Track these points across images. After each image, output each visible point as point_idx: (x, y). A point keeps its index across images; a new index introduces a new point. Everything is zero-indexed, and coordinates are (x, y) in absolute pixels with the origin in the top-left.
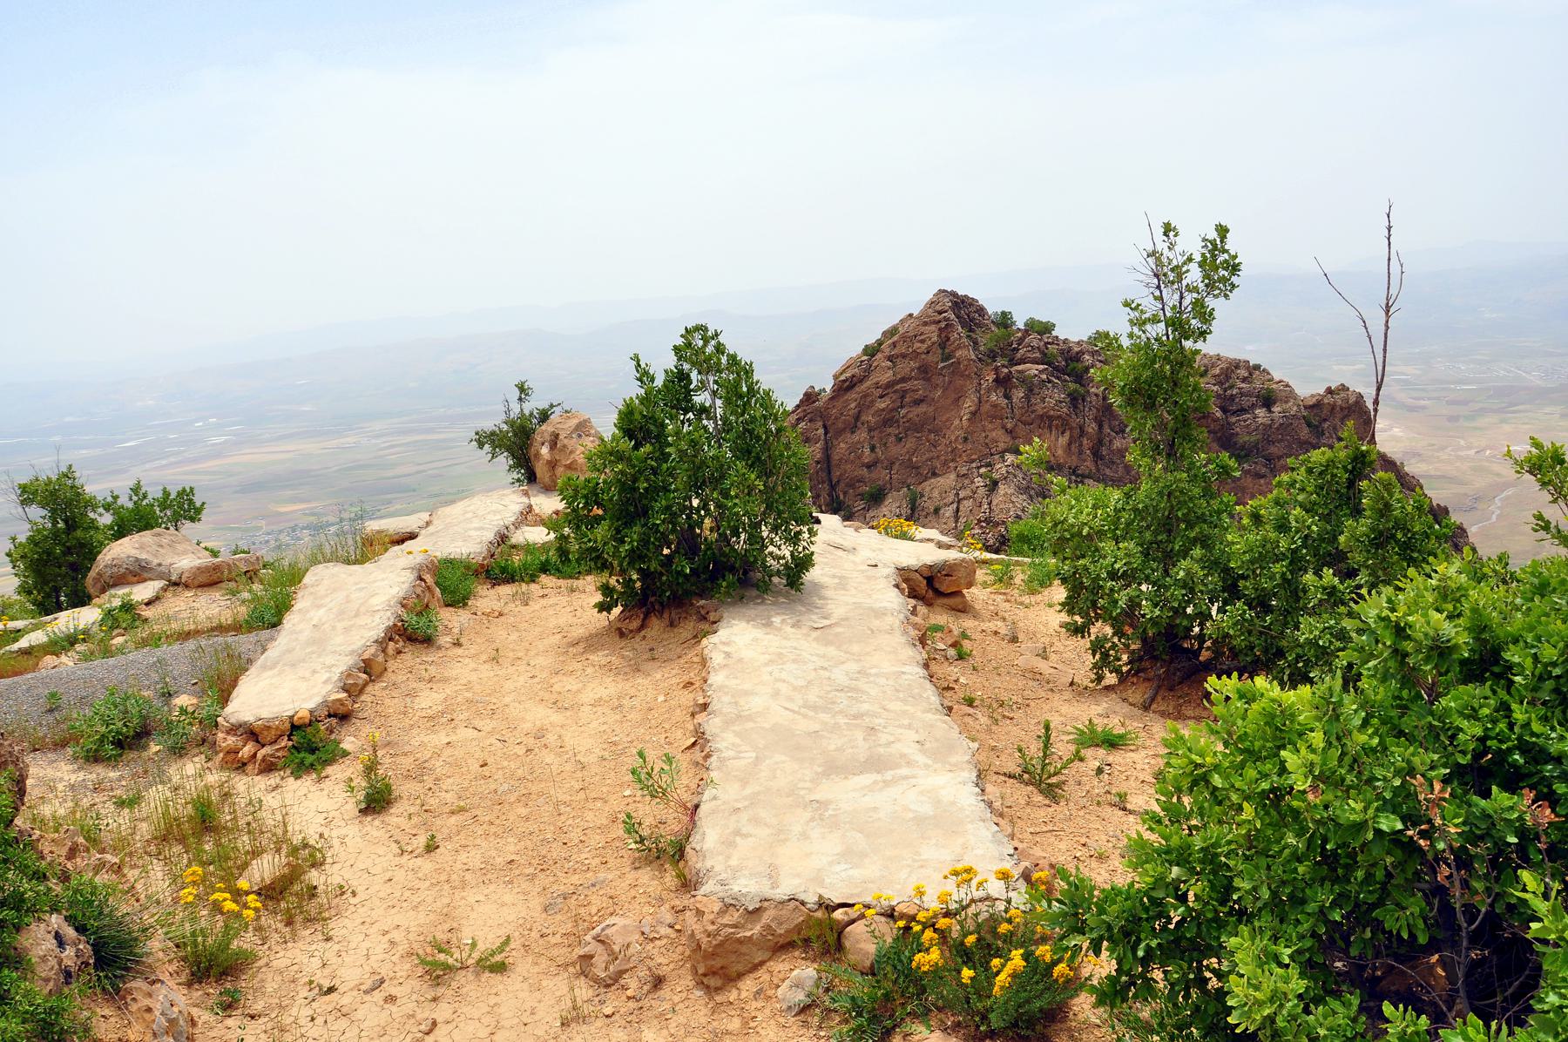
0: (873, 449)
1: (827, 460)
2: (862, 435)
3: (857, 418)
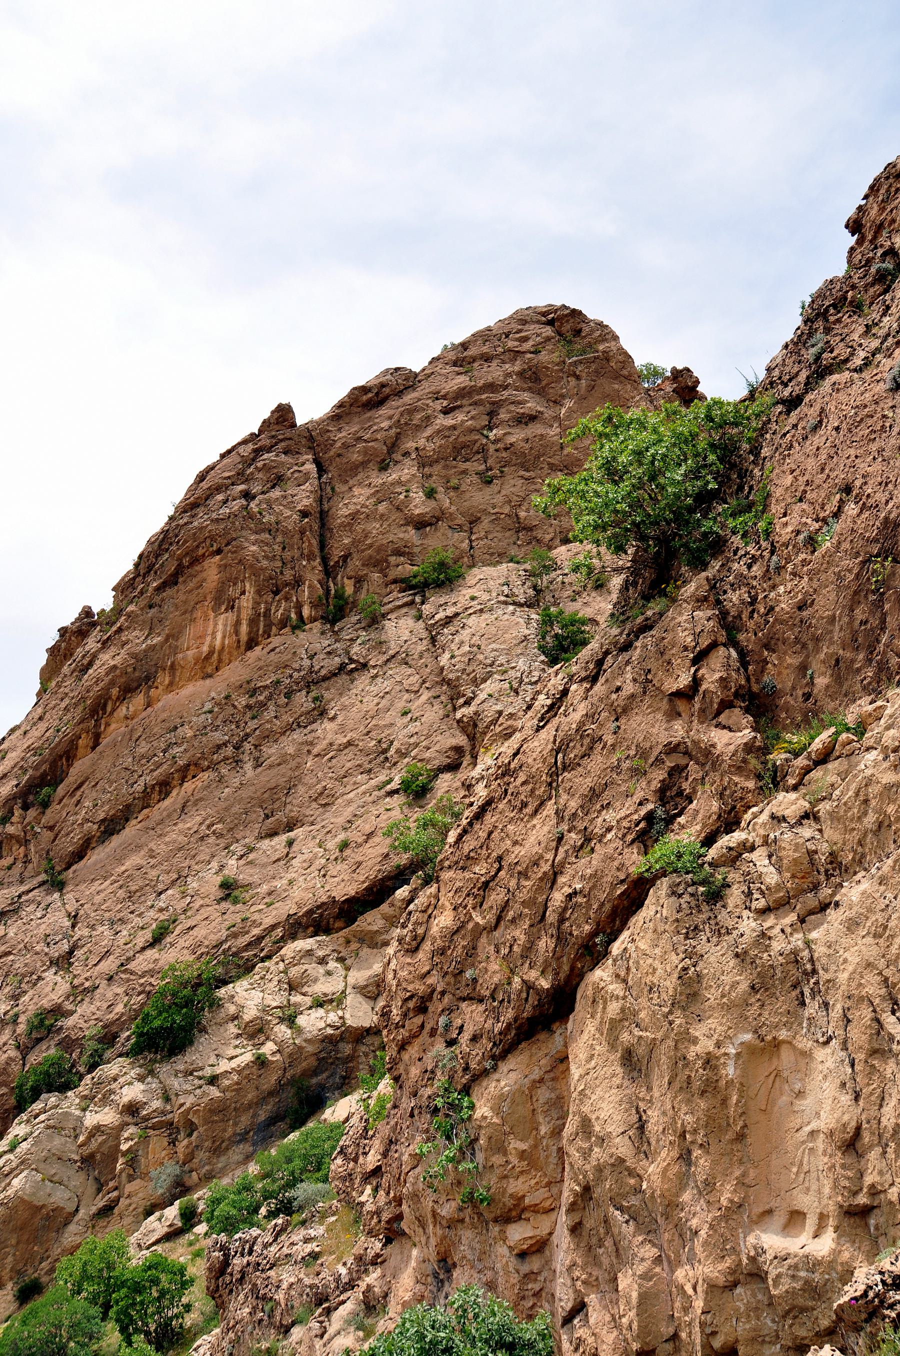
0: (430, 494)
1: (321, 516)
2: (406, 471)
3: (393, 446)
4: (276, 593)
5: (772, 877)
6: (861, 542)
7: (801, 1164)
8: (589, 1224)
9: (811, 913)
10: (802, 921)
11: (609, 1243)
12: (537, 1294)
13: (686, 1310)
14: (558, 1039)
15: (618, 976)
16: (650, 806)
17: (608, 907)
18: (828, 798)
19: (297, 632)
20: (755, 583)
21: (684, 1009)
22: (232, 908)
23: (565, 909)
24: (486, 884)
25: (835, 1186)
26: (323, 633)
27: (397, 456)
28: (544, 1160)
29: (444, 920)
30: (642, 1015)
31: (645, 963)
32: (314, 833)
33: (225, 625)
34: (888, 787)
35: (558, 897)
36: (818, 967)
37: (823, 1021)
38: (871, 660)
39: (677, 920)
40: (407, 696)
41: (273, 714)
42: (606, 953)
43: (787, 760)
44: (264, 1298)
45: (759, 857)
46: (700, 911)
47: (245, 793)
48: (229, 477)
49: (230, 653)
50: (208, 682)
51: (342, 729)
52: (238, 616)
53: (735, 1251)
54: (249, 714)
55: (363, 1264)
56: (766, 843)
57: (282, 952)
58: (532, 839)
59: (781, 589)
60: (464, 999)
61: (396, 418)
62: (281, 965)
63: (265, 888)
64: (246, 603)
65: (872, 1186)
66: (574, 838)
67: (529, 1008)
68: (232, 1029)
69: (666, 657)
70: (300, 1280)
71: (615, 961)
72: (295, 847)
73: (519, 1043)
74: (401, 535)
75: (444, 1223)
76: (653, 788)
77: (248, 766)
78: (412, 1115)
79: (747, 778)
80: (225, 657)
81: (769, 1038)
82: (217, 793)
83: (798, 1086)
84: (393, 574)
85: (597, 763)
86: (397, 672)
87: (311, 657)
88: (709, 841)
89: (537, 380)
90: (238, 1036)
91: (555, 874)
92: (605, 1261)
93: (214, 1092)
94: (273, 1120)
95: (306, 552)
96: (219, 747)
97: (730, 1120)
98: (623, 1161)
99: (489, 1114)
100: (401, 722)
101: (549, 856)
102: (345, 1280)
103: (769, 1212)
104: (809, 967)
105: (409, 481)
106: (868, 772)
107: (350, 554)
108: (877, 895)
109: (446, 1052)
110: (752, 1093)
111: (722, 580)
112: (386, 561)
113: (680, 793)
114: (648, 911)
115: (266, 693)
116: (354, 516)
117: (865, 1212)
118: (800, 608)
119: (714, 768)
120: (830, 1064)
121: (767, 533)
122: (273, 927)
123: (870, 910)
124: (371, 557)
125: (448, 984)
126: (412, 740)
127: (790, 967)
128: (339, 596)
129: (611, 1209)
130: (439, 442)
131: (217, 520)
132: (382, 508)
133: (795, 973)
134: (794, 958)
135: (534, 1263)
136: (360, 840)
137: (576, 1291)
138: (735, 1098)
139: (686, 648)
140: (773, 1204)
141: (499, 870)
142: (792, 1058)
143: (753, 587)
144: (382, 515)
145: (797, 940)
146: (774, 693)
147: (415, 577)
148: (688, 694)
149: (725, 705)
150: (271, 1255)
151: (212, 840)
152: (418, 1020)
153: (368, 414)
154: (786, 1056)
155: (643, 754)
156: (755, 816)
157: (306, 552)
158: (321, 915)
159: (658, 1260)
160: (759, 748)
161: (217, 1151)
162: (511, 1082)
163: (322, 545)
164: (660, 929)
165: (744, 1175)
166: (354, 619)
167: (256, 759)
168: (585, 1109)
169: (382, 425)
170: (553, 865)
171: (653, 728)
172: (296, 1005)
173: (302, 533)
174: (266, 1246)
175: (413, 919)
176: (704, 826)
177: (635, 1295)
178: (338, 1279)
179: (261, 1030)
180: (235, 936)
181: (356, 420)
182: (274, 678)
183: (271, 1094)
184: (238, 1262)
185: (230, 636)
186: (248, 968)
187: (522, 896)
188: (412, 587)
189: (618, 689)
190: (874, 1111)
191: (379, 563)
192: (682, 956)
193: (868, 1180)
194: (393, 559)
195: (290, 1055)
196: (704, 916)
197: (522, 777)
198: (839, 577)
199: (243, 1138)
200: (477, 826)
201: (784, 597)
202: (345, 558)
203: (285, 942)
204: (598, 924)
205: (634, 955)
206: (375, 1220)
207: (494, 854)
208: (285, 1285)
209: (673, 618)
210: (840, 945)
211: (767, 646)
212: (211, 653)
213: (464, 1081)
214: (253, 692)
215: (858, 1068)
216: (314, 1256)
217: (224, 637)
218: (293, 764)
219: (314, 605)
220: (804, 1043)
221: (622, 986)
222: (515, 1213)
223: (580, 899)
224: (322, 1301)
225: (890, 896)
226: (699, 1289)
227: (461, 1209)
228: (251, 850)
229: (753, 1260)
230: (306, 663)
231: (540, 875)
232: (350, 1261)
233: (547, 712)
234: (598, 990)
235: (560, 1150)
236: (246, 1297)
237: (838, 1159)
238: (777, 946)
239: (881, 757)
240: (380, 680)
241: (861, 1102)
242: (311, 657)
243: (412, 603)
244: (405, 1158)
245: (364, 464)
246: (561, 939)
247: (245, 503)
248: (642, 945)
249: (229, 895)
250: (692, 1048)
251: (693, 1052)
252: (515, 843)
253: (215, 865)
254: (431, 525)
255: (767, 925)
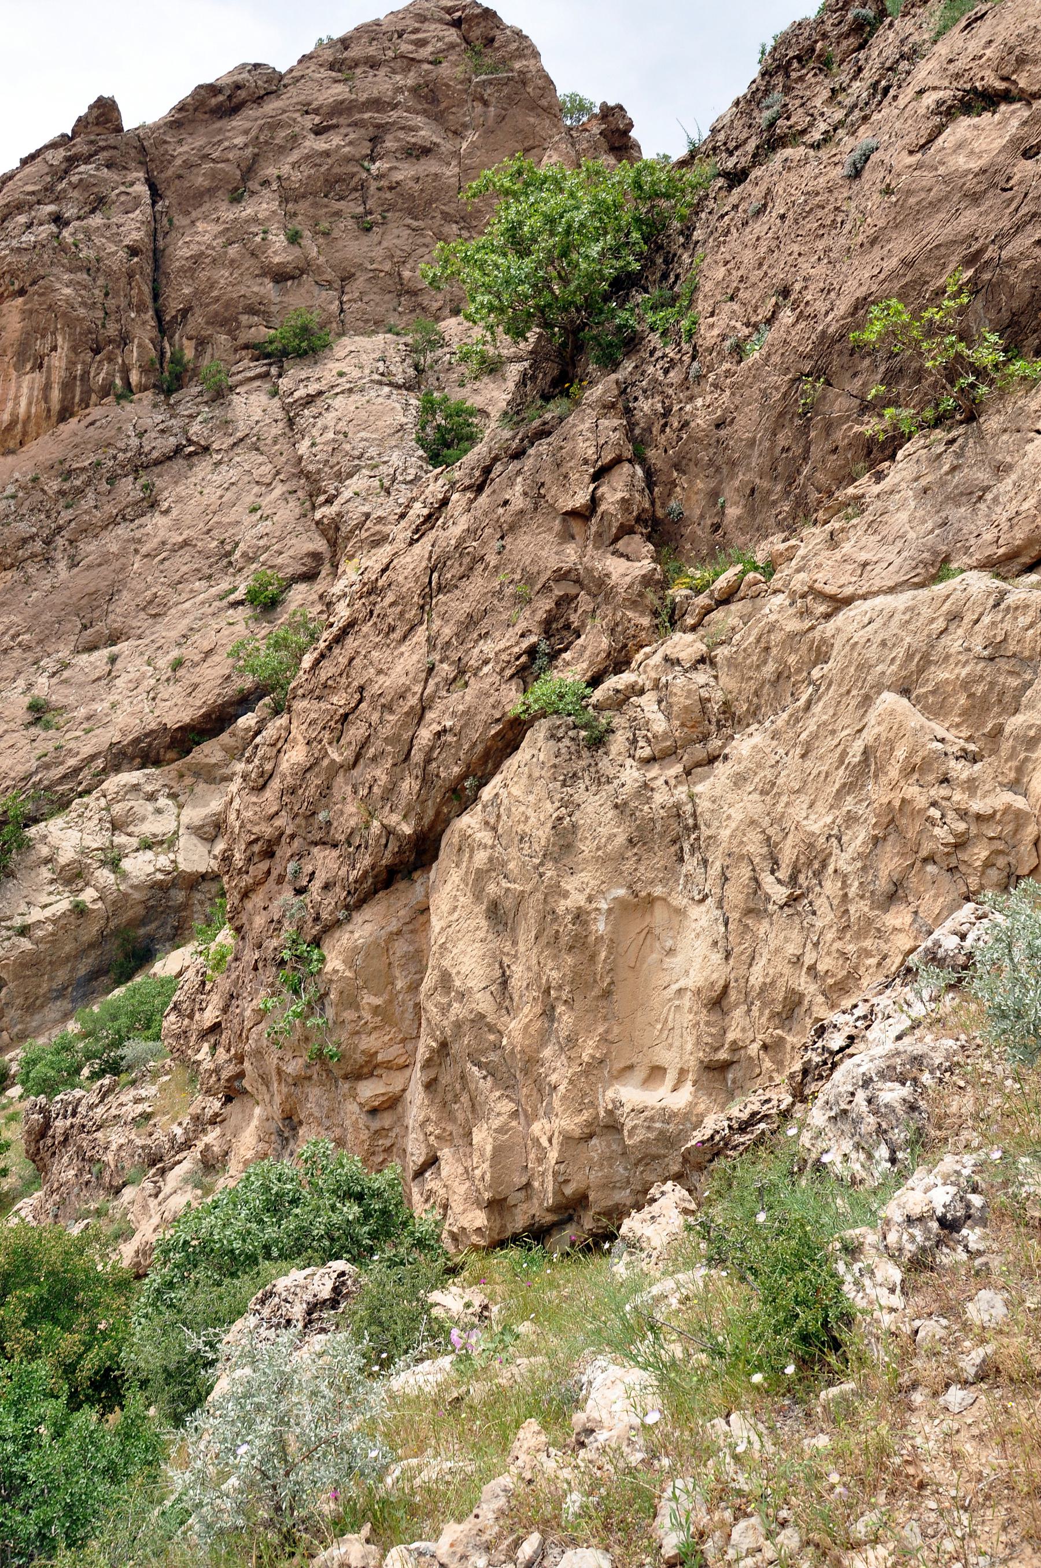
0: (294, 238)
1: (154, 255)
2: (263, 205)
4: (97, 351)
5: (659, 724)
6: (793, 357)
7: (666, 1021)
8: (445, 1079)
9: (698, 765)
10: (688, 773)
11: (465, 1098)
12: (388, 1150)
13: (540, 1161)
14: (419, 889)
15: (487, 823)
16: (533, 639)
17: (480, 748)
18: (727, 642)
19: (123, 402)
20: (670, 392)
21: (556, 861)
22: (43, 735)
23: (432, 749)
24: (345, 717)
25: (698, 1043)
26: (155, 406)
27: (253, 185)
28: (401, 1016)
29: (296, 755)
30: (511, 866)
31: (517, 811)
32: (142, 648)
33: (31, 389)
34: (792, 636)
35: (425, 735)
36: (700, 821)
37: (700, 879)
38: (788, 493)
39: (555, 766)
40: (256, 489)
41: (92, 503)
42: (476, 799)
43: (687, 597)
44: (91, 1160)
45: (648, 702)
46: (579, 757)
47: (58, 598)
48: (33, 193)
49: (37, 424)
50: (10, 459)
51: (177, 525)
52: (48, 378)
53: (593, 1104)
54: (62, 502)
55: (200, 1123)
56: (656, 686)
57: (104, 786)
58: (399, 668)
59: (699, 402)
60: (316, 844)
61: (253, 133)
62: (103, 802)
63: (82, 712)
64: (58, 361)
65: (734, 1042)
66: (446, 669)
67: (388, 854)
68: (45, 873)
69: (563, 470)
70: (131, 1141)
71: (485, 807)
72: (119, 665)
73: (376, 892)
74: (256, 289)
75: (290, 1080)
76: (537, 618)
77: (62, 566)
78: (255, 969)
79: (642, 614)
80: (32, 428)
81: (643, 894)
82: (23, 597)
83: (669, 944)
84: (246, 336)
85: (477, 586)
86: (245, 458)
87: (140, 435)
88: (595, 682)
89: (434, 101)
90: (52, 882)
91: (423, 709)
92: (460, 1116)
93: (26, 944)
94: (95, 975)
95: (135, 301)
96: (24, 541)
97: (596, 975)
98: (482, 1016)
99: (340, 967)
100: (248, 519)
101: (418, 688)
102: (180, 1139)
103: (631, 1067)
104: (691, 822)
105: (267, 219)
106: (772, 618)
107: (191, 308)
108: (768, 750)
109: (295, 900)
110: (621, 950)
111: (633, 384)
112: (236, 320)
113: (567, 626)
114: (522, 755)
115: (84, 477)
116: (197, 259)
117: (724, 1067)
118: (718, 426)
119: (607, 600)
120: (704, 922)
121: (690, 334)
122: (93, 757)
123: (759, 765)
124: (217, 314)
125: (299, 826)
126: (261, 543)
127: (672, 821)
128: (176, 360)
129: (469, 1065)
130: (307, 171)
131: (19, 250)
132: (233, 251)
133: (676, 828)
134: (676, 812)
135: (386, 1120)
136: (196, 659)
137: (429, 1146)
138: (603, 955)
139: (586, 462)
140: (634, 1060)
141: (360, 701)
142: (666, 915)
143: (669, 397)
144: (232, 261)
145: (681, 793)
146: (680, 519)
147: (271, 342)
148: (584, 514)
149: (626, 530)
150: (97, 1117)
151: (17, 653)
152: (264, 866)
153: (218, 125)
154: (660, 913)
155: (529, 579)
156: (647, 657)
157: (135, 301)
158: (150, 745)
159: (515, 1114)
160: (658, 582)
161: (31, 1008)
162: (366, 934)
163: (156, 297)
164: (536, 774)
165: (607, 1032)
166: (195, 390)
167: (71, 557)
168: (446, 963)
169: (236, 141)
170: (421, 699)
171: (543, 550)
172: (119, 846)
173: (130, 276)
174: (91, 1107)
175: (260, 753)
176: (591, 664)
177: (489, 1148)
178: (173, 1139)
179: (79, 875)
180: (47, 767)
181: (202, 130)
182: (93, 458)
183: (92, 946)
184: (60, 1125)
185: (38, 403)
186: (63, 805)
187: (385, 731)
188: (268, 356)
189: (506, 503)
190: (742, 971)
191: (226, 321)
192: (557, 804)
193: (731, 1036)
194: (244, 319)
195: (114, 903)
196: (583, 763)
197: (390, 598)
198: (765, 394)
199: (60, 994)
200: (336, 651)
201: (700, 411)
202: (185, 312)
203: (108, 776)
204: (468, 767)
205: (506, 802)
206: (214, 1078)
207: (356, 684)
208: (114, 1147)
209: (574, 426)
210: (727, 803)
211: (677, 467)
212: (13, 423)
213: (314, 932)
214: (68, 475)
215: (731, 927)
216: (147, 1116)
217: (30, 404)
218: (117, 565)
219: (144, 370)
220: (679, 900)
221: (491, 834)
222: (367, 1069)
223: (449, 738)
224: (156, 1162)
225: (781, 751)
226: (555, 1141)
227: (308, 1066)
228: (65, 666)
229: (610, 1113)
230: (134, 442)
231: (406, 709)
232: (186, 1120)
233: (423, 523)
234: (465, 837)
235: (417, 1006)
236: (71, 1159)
237: (704, 1016)
238: (660, 798)
239: (787, 602)
240: (224, 468)
241: (731, 961)
242: (140, 435)
243: (266, 375)
244: (248, 1013)
245: (210, 192)
246: (426, 780)
247: (55, 230)
248: (515, 791)
249: (39, 719)
250: (562, 902)
251: (563, 906)
252: (380, 672)
253: (21, 683)
254: (293, 278)
255: (650, 775)
